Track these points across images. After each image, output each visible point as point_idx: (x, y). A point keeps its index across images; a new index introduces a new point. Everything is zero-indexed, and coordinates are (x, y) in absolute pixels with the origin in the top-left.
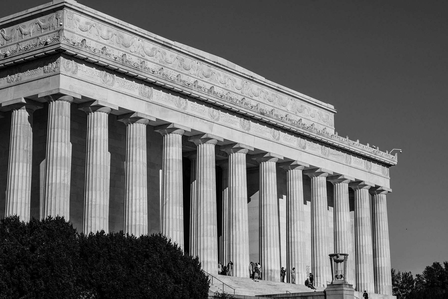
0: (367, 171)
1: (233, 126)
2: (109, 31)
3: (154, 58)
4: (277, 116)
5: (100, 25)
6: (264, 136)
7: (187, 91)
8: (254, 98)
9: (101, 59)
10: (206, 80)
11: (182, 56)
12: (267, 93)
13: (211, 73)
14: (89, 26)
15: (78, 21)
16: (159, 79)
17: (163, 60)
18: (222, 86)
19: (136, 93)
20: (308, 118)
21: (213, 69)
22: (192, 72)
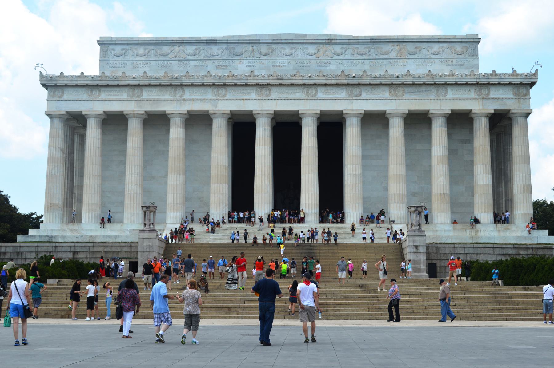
0: (481, 97)
1: (245, 97)
2: (145, 49)
3: (197, 56)
5: (136, 47)
6: (292, 97)
9: (79, 82)
10: (265, 58)
11: (232, 46)
12: (358, 48)
13: (270, 51)
14: (124, 51)
15: (114, 50)
16: (141, 82)
17: (209, 55)
18: (288, 57)
20: (428, 57)
21: (274, 46)
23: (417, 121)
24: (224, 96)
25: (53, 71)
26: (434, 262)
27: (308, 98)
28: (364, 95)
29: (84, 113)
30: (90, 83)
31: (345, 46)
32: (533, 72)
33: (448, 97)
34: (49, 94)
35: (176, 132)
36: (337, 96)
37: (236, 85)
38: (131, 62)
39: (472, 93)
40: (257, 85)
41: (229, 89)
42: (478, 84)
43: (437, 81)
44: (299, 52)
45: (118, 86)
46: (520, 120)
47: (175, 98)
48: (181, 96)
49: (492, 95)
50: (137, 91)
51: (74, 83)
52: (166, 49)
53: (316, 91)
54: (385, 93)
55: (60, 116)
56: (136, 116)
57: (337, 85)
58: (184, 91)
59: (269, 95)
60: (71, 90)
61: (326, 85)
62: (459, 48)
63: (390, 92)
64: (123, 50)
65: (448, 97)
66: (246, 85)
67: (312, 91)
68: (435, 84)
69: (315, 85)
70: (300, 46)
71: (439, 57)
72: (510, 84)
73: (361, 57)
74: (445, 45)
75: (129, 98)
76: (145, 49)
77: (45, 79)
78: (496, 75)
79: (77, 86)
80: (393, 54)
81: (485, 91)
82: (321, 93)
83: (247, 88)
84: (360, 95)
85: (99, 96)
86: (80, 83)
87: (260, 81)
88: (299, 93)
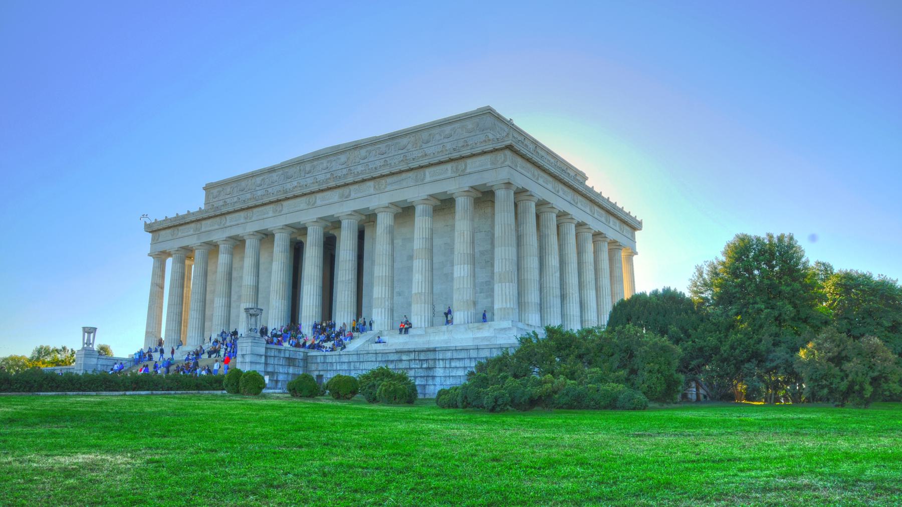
7: (218, 213)
8: (362, 162)
19: (191, 232)
21: (315, 163)
26: (321, 373)
28: (353, 195)
31: (369, 148)
34: (153, 240)
41: (255, 210)
42: (451, 160)
49: (468, 171)
52: (243, 184)
62: (470, 125)
68: (411, 170)
71: (451, 139)
72: (484, 153)
73: (383, 157)
74: (457, 125)
81: (461, 165)
84: (349, 195)
86: (165, 225)
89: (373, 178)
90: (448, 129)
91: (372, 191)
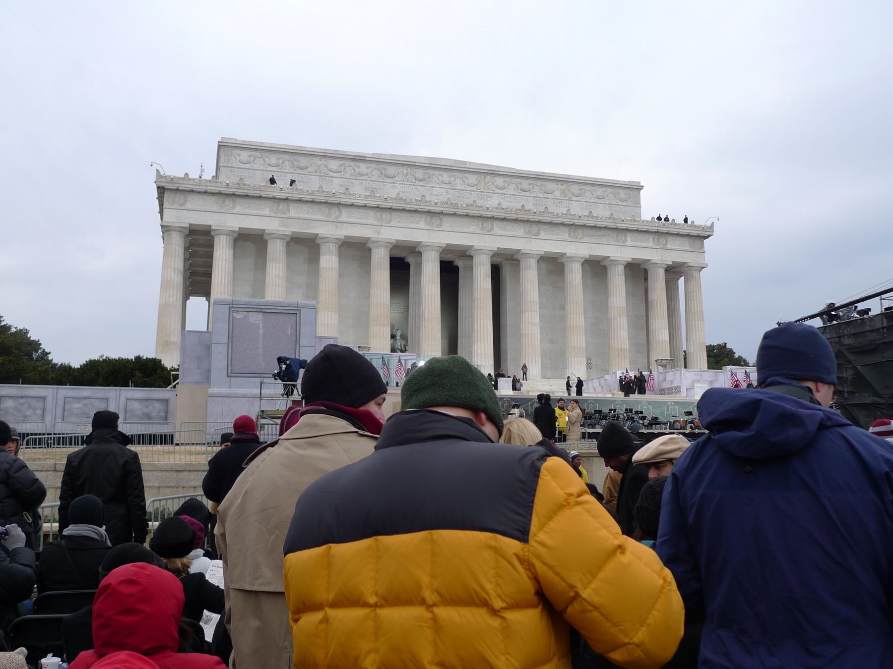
4: (481, 207)
5: (267, 155)
8: (498, 191)
10: (421, 183)
12: (521, 184)
18: (447, 186)
21: (431, 172)
22: (398, 178)
23: (597, 268)
24: (389, 222)
25: (174, 170)
27: (484, 232)
28: (543, 235)
29: (213, 228)
30: (224, 190)
31: (507, 179)
32: (709, 224)
33: (627, 244)
35: (329, 261)
36: (515, 233)
37: (403, 210)
38: (260, 172)
39: (650, 241)
40: (429, 212)
41: (394, 214)
43: (620, 226)
44: (458, 181)
45: (260, 197)
46: (695, 273)
47: (330, 219)
48: (337, 218)
49: (669, 246)
50: (282, 206)
51: (203, 188)
52: (304, 161)
53: (492, 225)
54: (564, 234)
55: (181, 230)
56: (282, 237)
57: (516, 220)
58: (340, 211)
59: (440, 226)
60: (196, 198)
61: (504, 219)
62: (622, 194)
63: (570, 234)
64: (250, 156)
65: (627, 244)
66: (416, 211)
67: (488, 225)
68: (616, 229)
69: (493, 218)
70: (460, 175)
71: (602, 201)
73: (525, 194)
74: (609, 190)
75: (273, 214)
76: (279, 159)
77: (163, 180)
78: (675, 224)
79: (205, 192)
80: (557, 194)
81: (663, 240)
82: (498, 228)
83: (415, 215)
84: (539, 234)
85: (233, 208)
87: (432, 208)
88: (473, 227)
89: (572, 226)
90: (599, 191)
91: (566, 237)
